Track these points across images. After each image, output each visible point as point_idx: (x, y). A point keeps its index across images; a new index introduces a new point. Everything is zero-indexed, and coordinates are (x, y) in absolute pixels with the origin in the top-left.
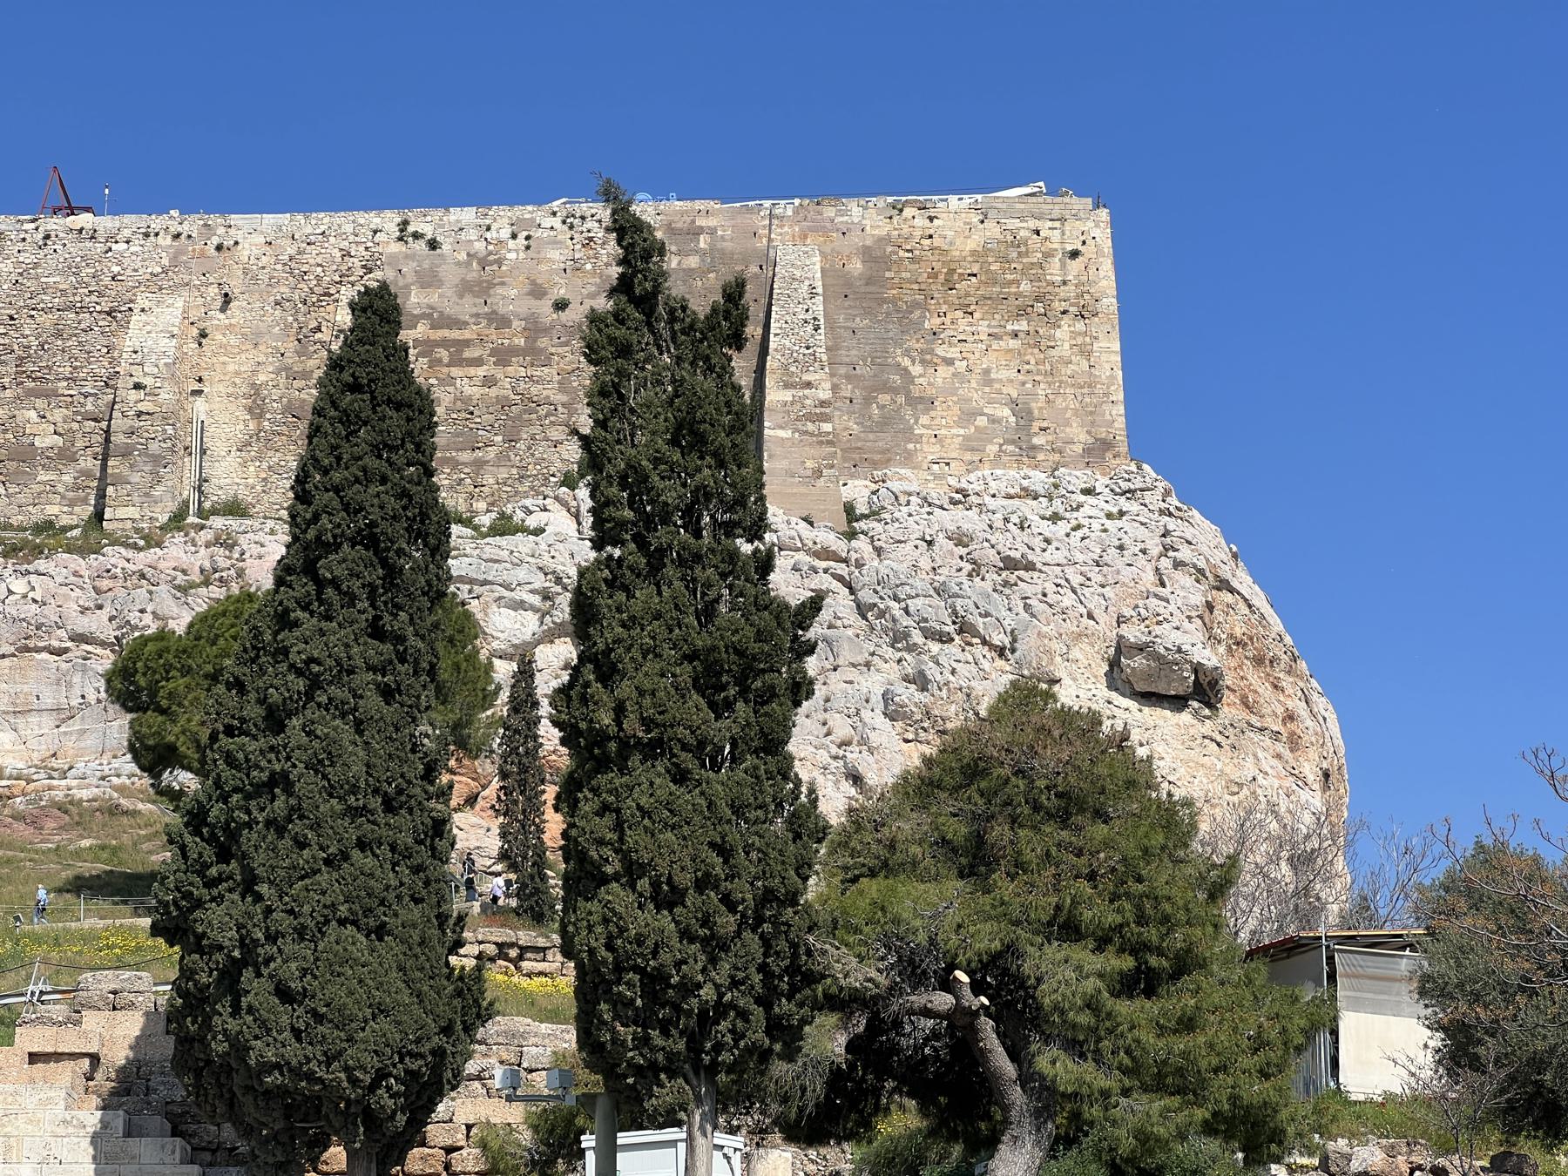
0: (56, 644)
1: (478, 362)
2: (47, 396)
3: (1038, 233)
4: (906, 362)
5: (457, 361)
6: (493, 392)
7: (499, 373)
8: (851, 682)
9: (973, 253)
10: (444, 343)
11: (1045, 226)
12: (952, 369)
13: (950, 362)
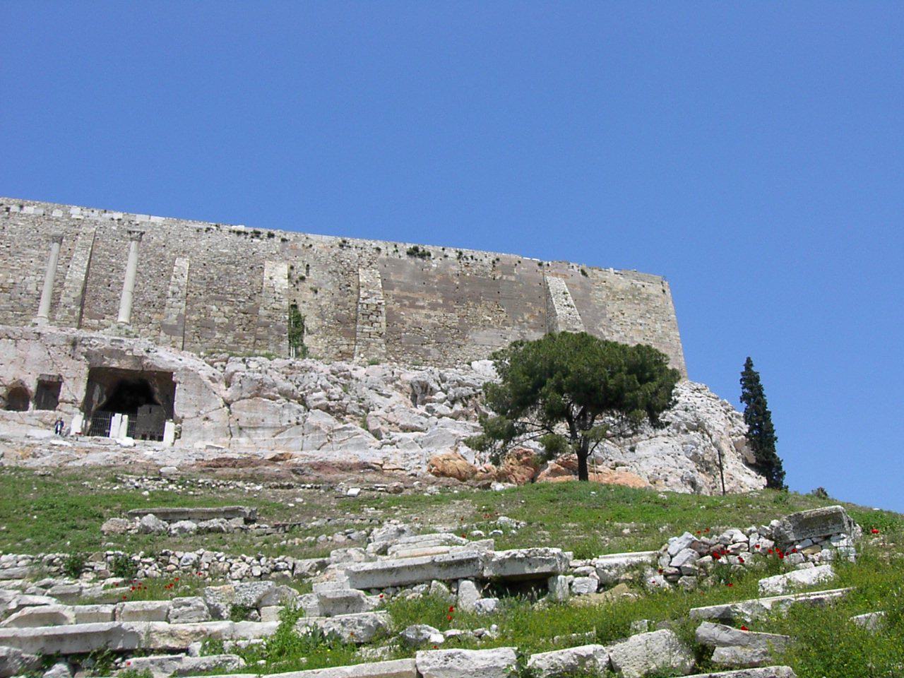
0: (272, 394)
1: (423, 307)
2: (221, 300)
3: (644, 286)
4: (601, 330)
5: (413, 306)
6: (430, 321)
7: (432, 313)
8: (667, 443)
9: (622, 291)
10: (406, 297)
11: (646, 284)
12: (619, 335)
13: (618, 332)
